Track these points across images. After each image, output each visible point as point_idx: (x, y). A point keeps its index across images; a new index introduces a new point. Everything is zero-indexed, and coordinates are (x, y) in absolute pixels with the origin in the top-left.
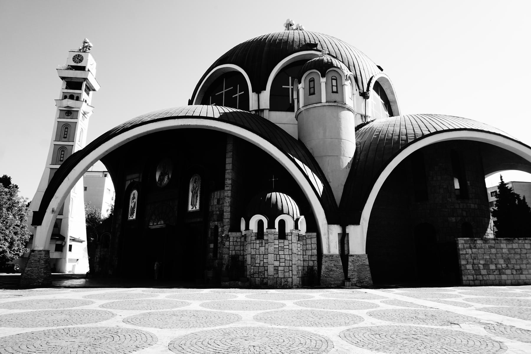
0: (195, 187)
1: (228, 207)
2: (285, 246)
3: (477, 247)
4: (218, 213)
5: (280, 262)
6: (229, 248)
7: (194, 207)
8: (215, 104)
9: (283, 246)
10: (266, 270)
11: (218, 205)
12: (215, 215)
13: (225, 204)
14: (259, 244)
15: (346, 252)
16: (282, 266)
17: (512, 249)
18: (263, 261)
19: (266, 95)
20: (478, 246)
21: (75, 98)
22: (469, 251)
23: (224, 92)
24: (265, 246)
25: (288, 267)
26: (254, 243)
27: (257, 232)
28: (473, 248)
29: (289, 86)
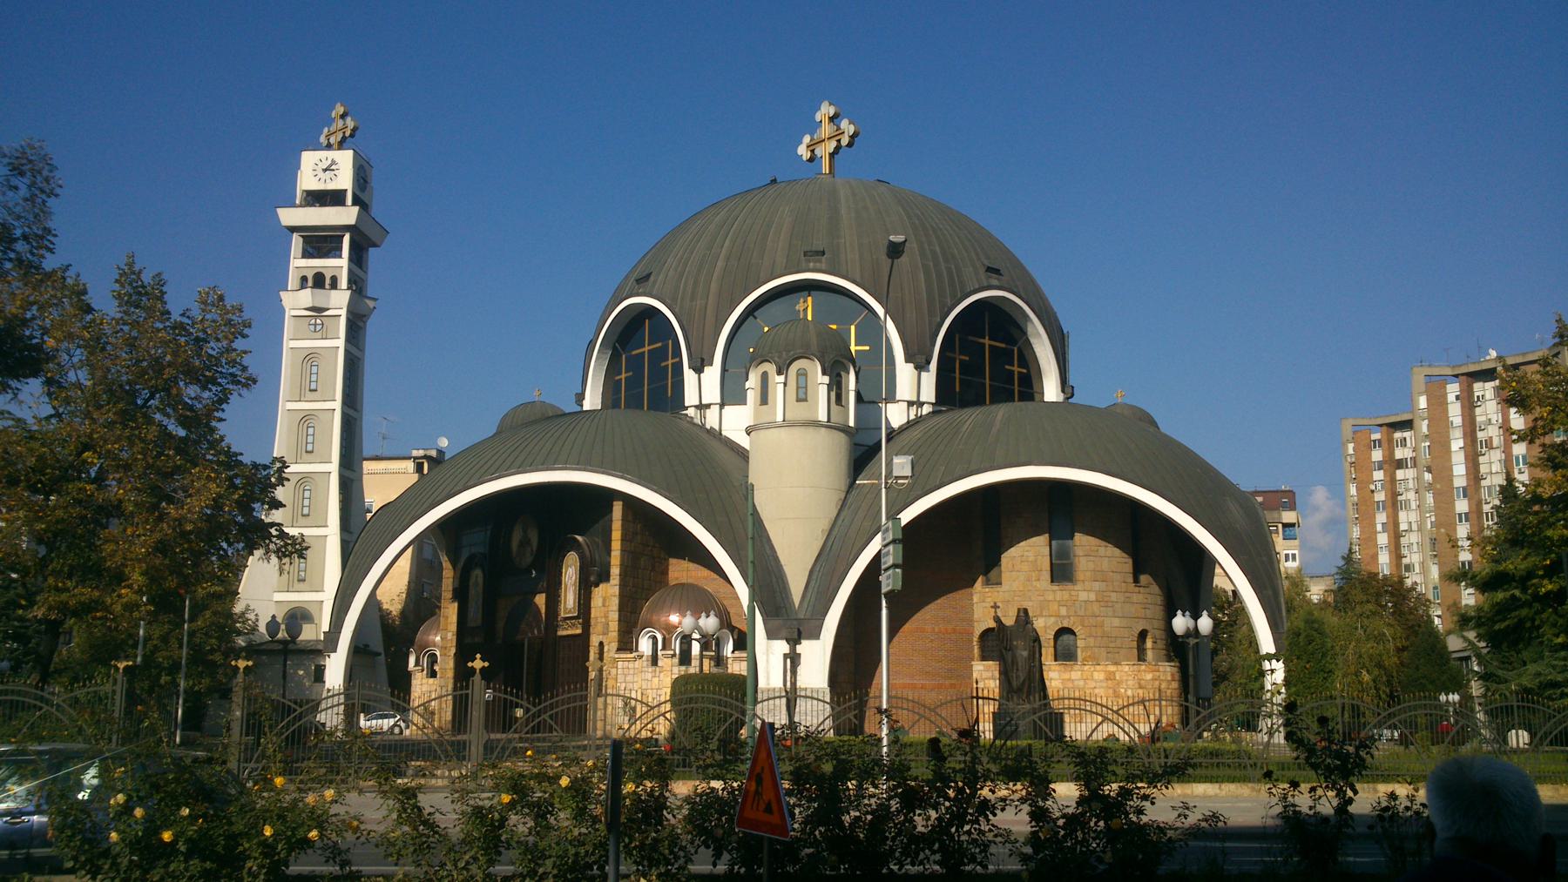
4: (603, 620)
13: (610, 608)
17: (1069, 680)
19: (712, 374)
21: (328, 281)
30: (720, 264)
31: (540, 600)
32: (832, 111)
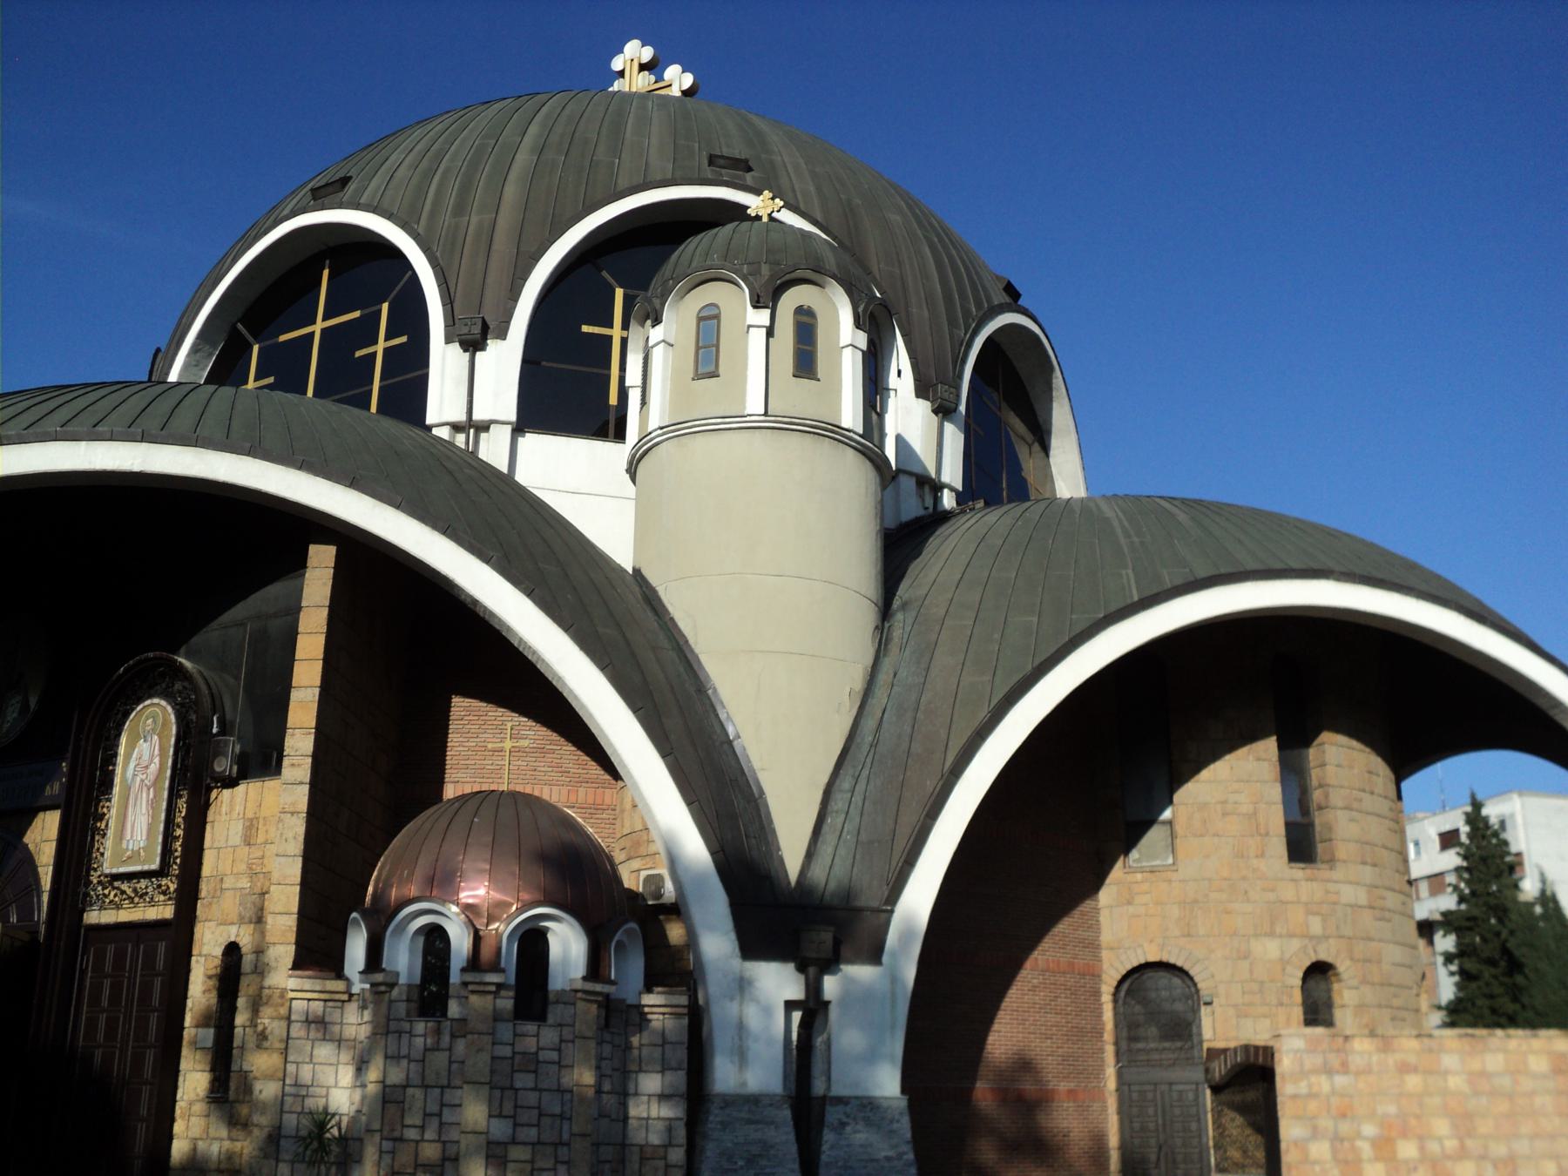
0: (146, 757)
1: (291, 859)
2: (541, 1053)
3: (1352, 1067)
4: (245, 883)
5: (515, 1125)
6: (286, 1048)
8: (271, 380)
9: (534, 1050)
10: (449, 1159)
12: (228, 894)
14: (425, 1035)
15: (818, 1087)
16: (527, 1140)
18: (440, 1115)
20: (1356, 1061)
22: (1324, 1084)
23: (318, 327)
24: (450, 1049)
25: (550, 1150)
26: (400, 1033)
27: (417, 980)
28: (1338, 1072)
29: (612, 327)
30: (523, 158)
31: (44, 834)
32: (647, 54)
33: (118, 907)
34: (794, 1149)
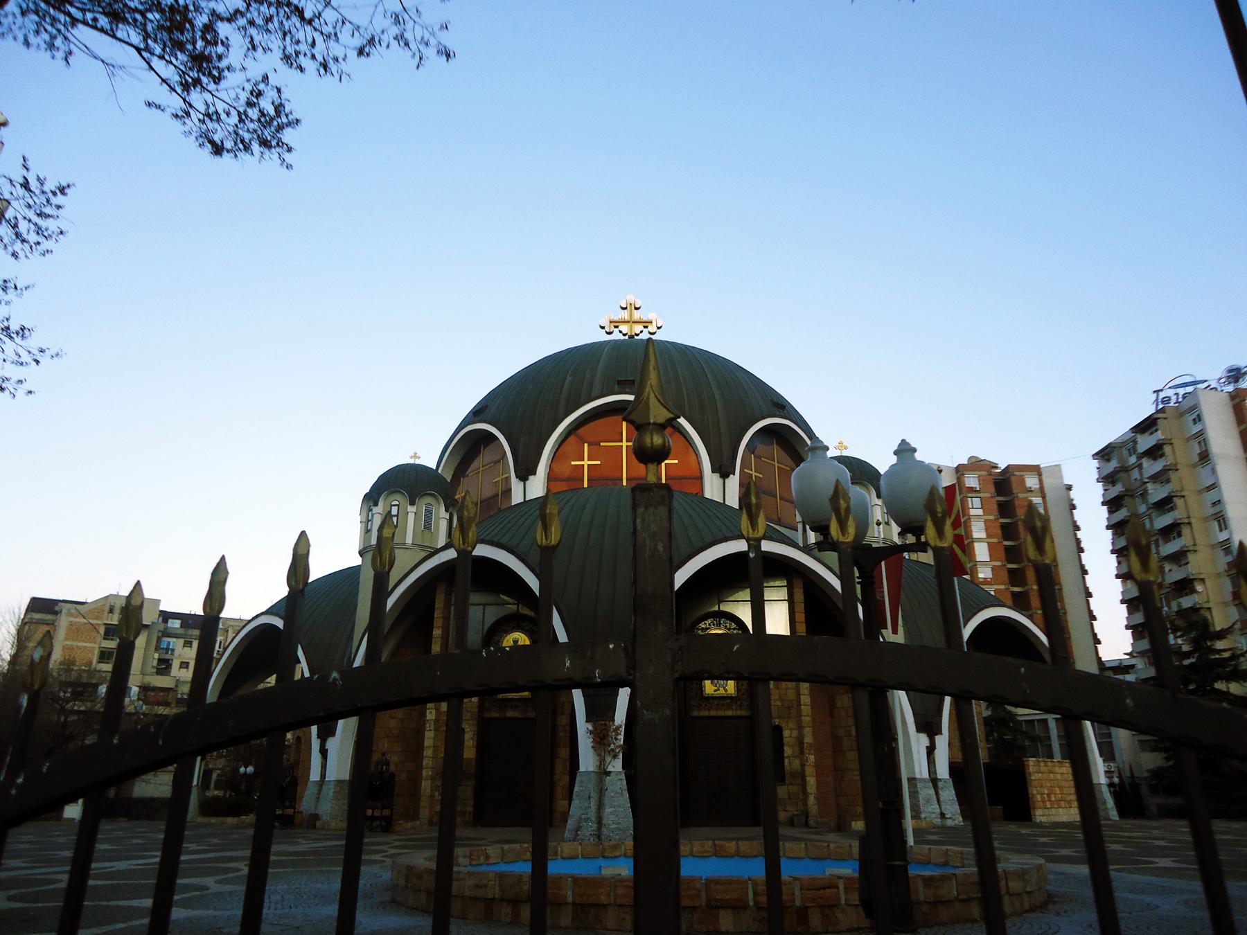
4: (779, 703)
7: (721, 689)
11: (777, 691)
19: (734, 482)
33: (709, 710)
34: (935, 796)
